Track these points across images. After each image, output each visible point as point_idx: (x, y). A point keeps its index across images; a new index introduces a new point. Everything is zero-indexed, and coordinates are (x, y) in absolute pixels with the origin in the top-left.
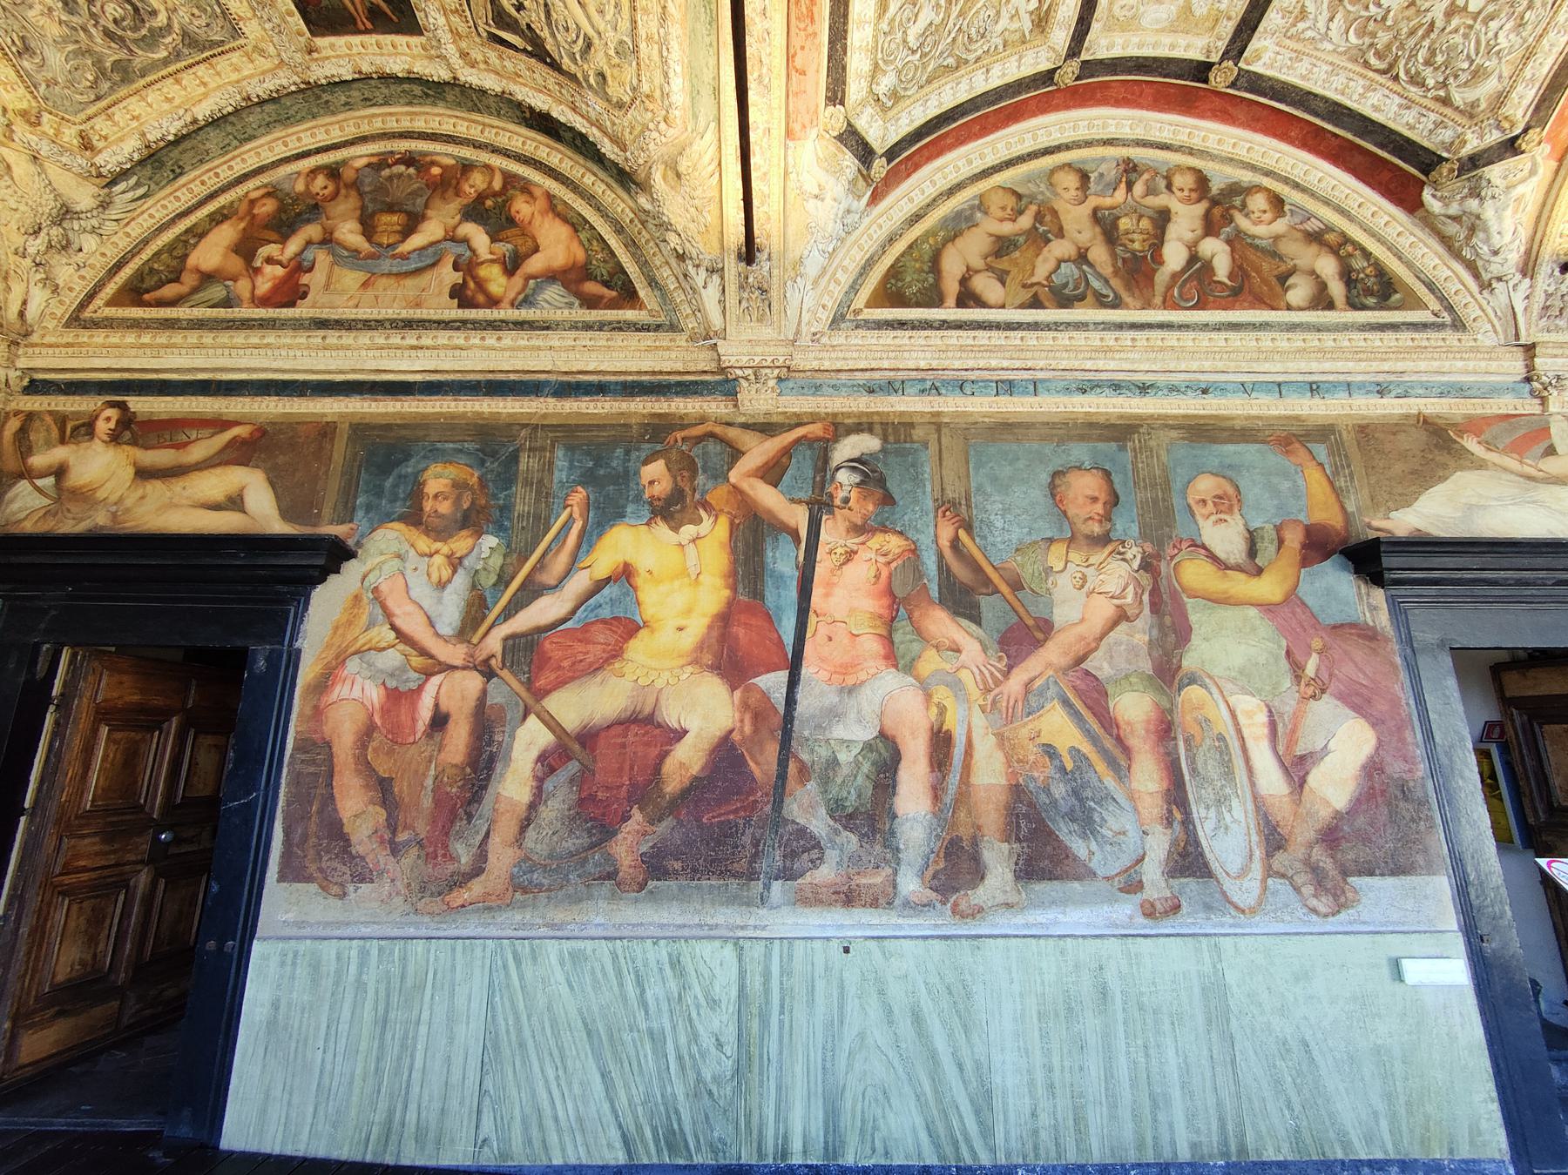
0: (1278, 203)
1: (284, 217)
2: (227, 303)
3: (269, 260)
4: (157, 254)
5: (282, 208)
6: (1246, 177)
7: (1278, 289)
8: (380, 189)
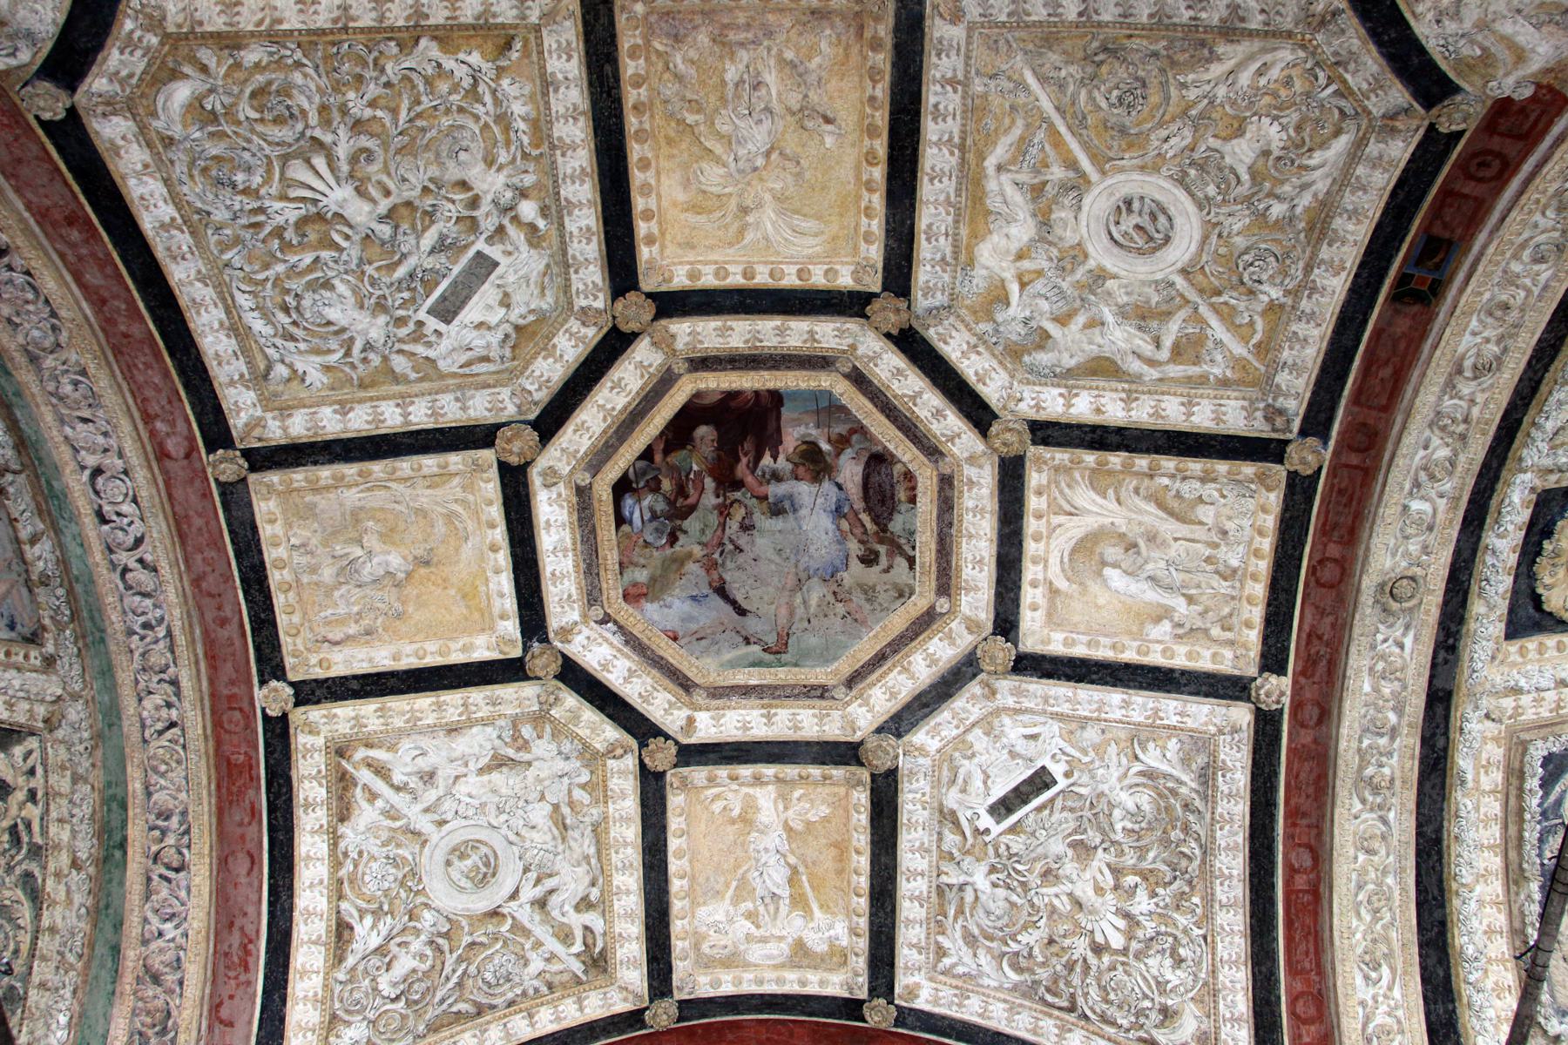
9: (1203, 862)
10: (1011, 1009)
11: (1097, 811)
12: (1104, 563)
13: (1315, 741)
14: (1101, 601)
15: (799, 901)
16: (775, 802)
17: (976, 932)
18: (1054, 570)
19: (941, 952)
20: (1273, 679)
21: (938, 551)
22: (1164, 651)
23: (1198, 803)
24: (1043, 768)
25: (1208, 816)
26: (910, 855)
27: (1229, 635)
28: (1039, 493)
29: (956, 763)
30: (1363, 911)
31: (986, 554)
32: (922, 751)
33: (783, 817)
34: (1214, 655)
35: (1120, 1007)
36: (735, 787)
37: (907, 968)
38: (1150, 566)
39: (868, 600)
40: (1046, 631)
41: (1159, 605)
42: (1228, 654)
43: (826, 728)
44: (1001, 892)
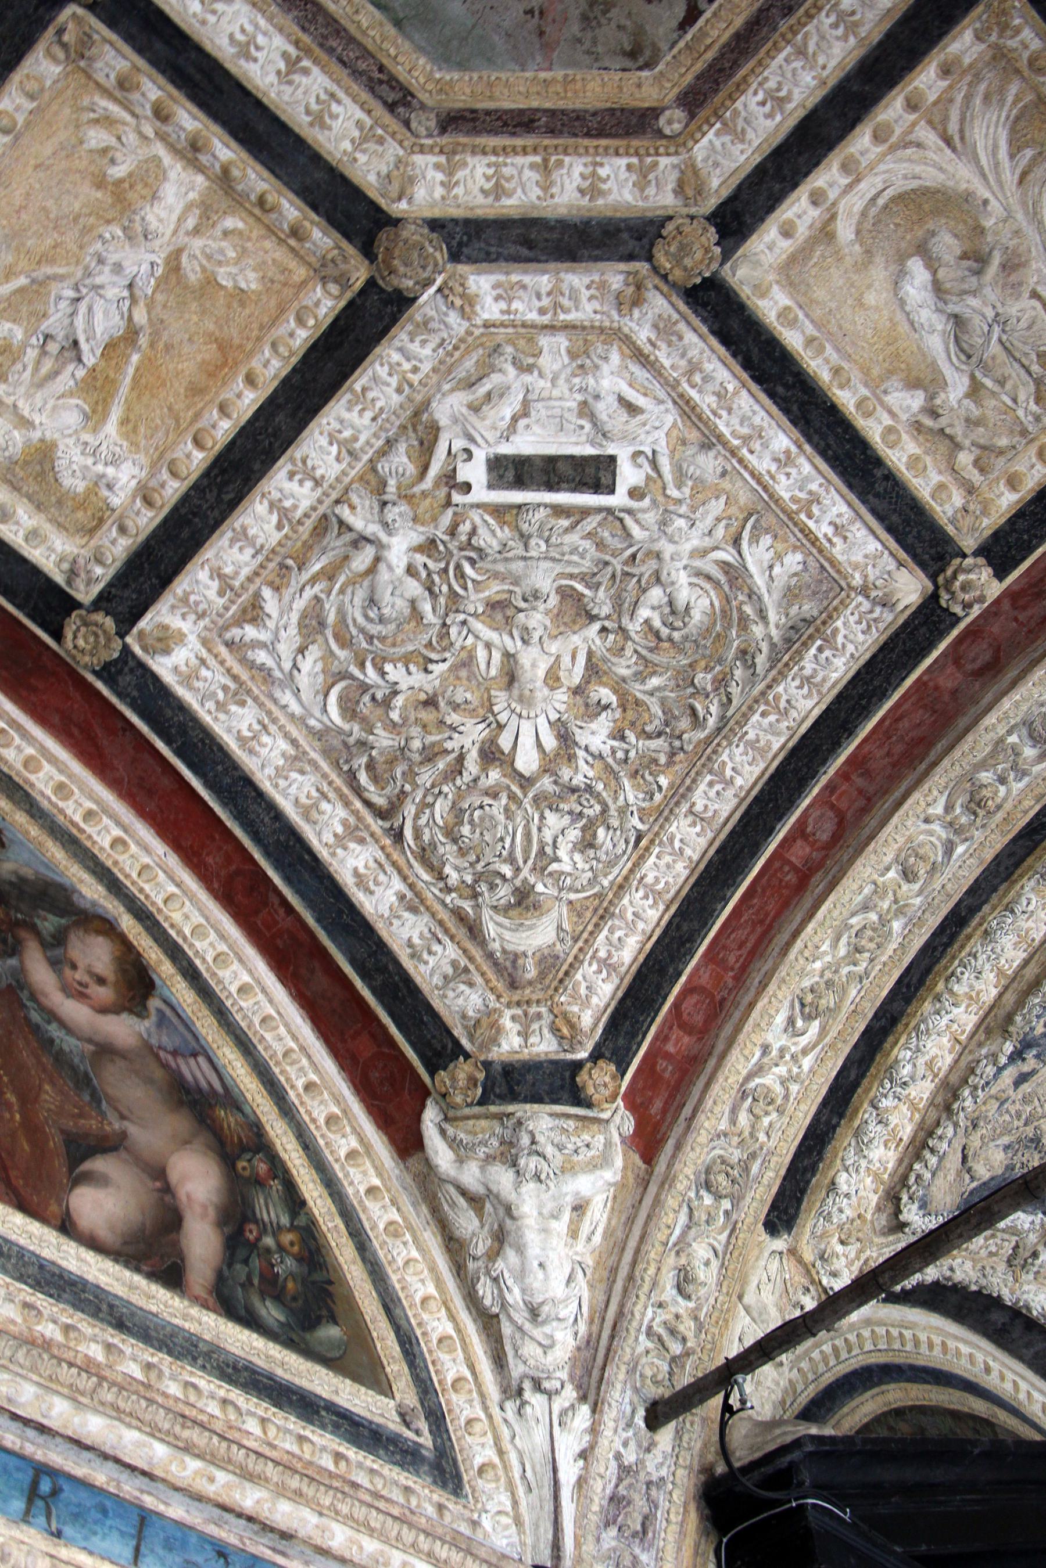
0: (136, 985)
6: (91, 891)
7: (59, 1165)
9: (708, 741)
10: (296, 758)
11: (632, 572)
12: (922, 249)
13: (954, 693)
14: (870, 298)
15: (97, 390)
16: (189, 207)
17: (331, 618)
18: (855, 202)
19: (253, 613)
20: (985, 574)
21: (737, 36)
22: (889, 430)
23: (761, 660)
24: (612, 459)
25: (760, 687)
26: (323, 441)
27: (976, 477)
28: (946, 71)
29: (498, 361)
30: (844, 940)
31: (797, 96)
32: (468, 305)
33: (182, 239)
34: (941, 487)
35: (462, 852)
36: (149, 131)
37: (185, 600)
38: (974, 302)
39: (585, 18)
40: (772, 277)
41: (934, 366)
42: (958, 499)
43: (362, 158)
44: (414, 588)
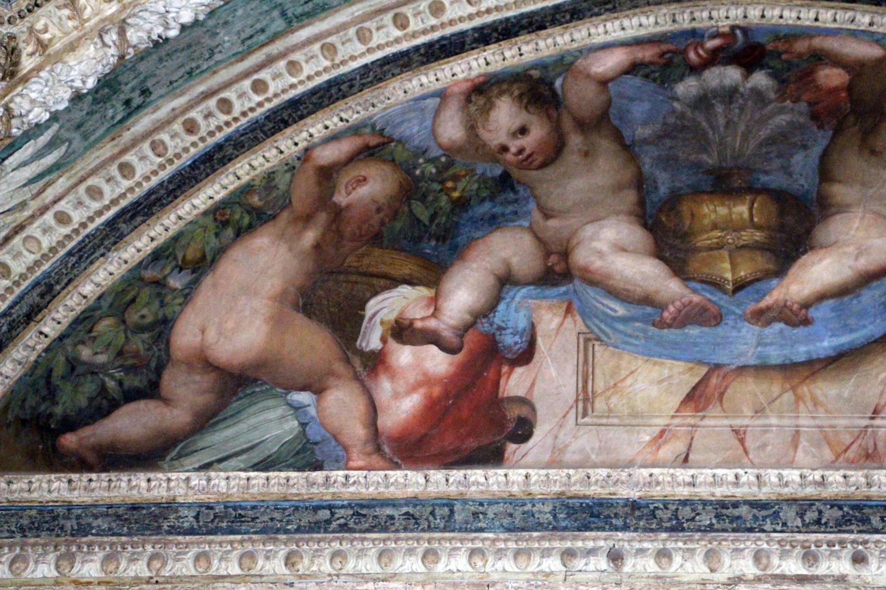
1: (422, 212)
2: (305, 455)
3: (403, 331)
4: (85, 321)
5: (410, 189)
8: (676, 130)
